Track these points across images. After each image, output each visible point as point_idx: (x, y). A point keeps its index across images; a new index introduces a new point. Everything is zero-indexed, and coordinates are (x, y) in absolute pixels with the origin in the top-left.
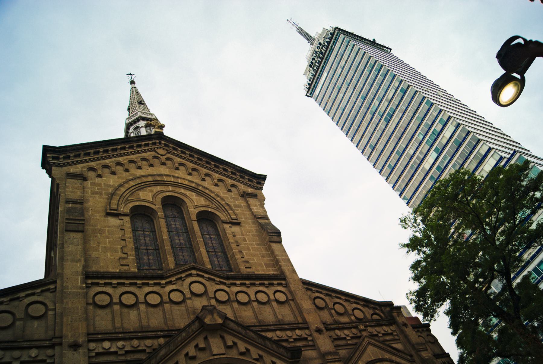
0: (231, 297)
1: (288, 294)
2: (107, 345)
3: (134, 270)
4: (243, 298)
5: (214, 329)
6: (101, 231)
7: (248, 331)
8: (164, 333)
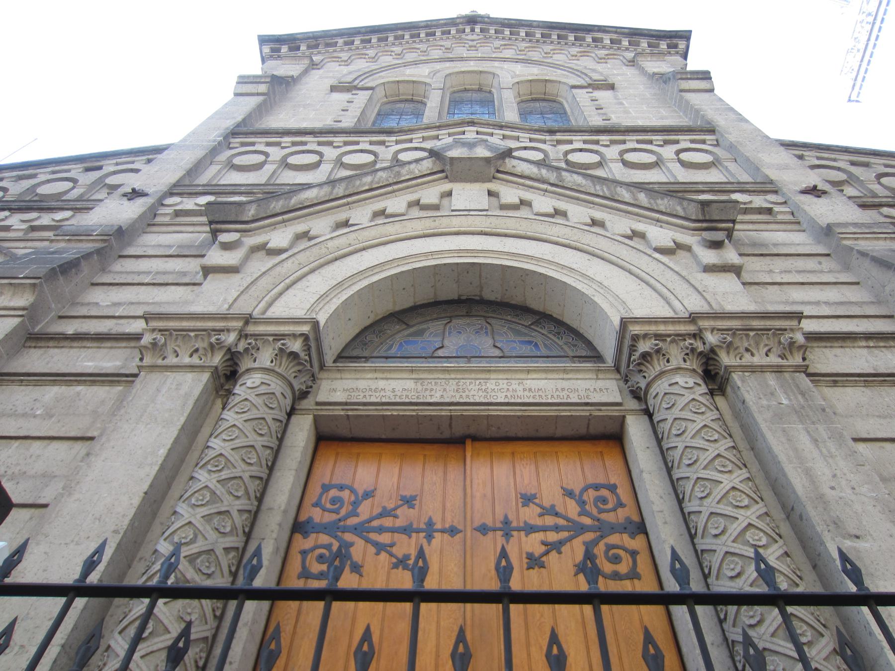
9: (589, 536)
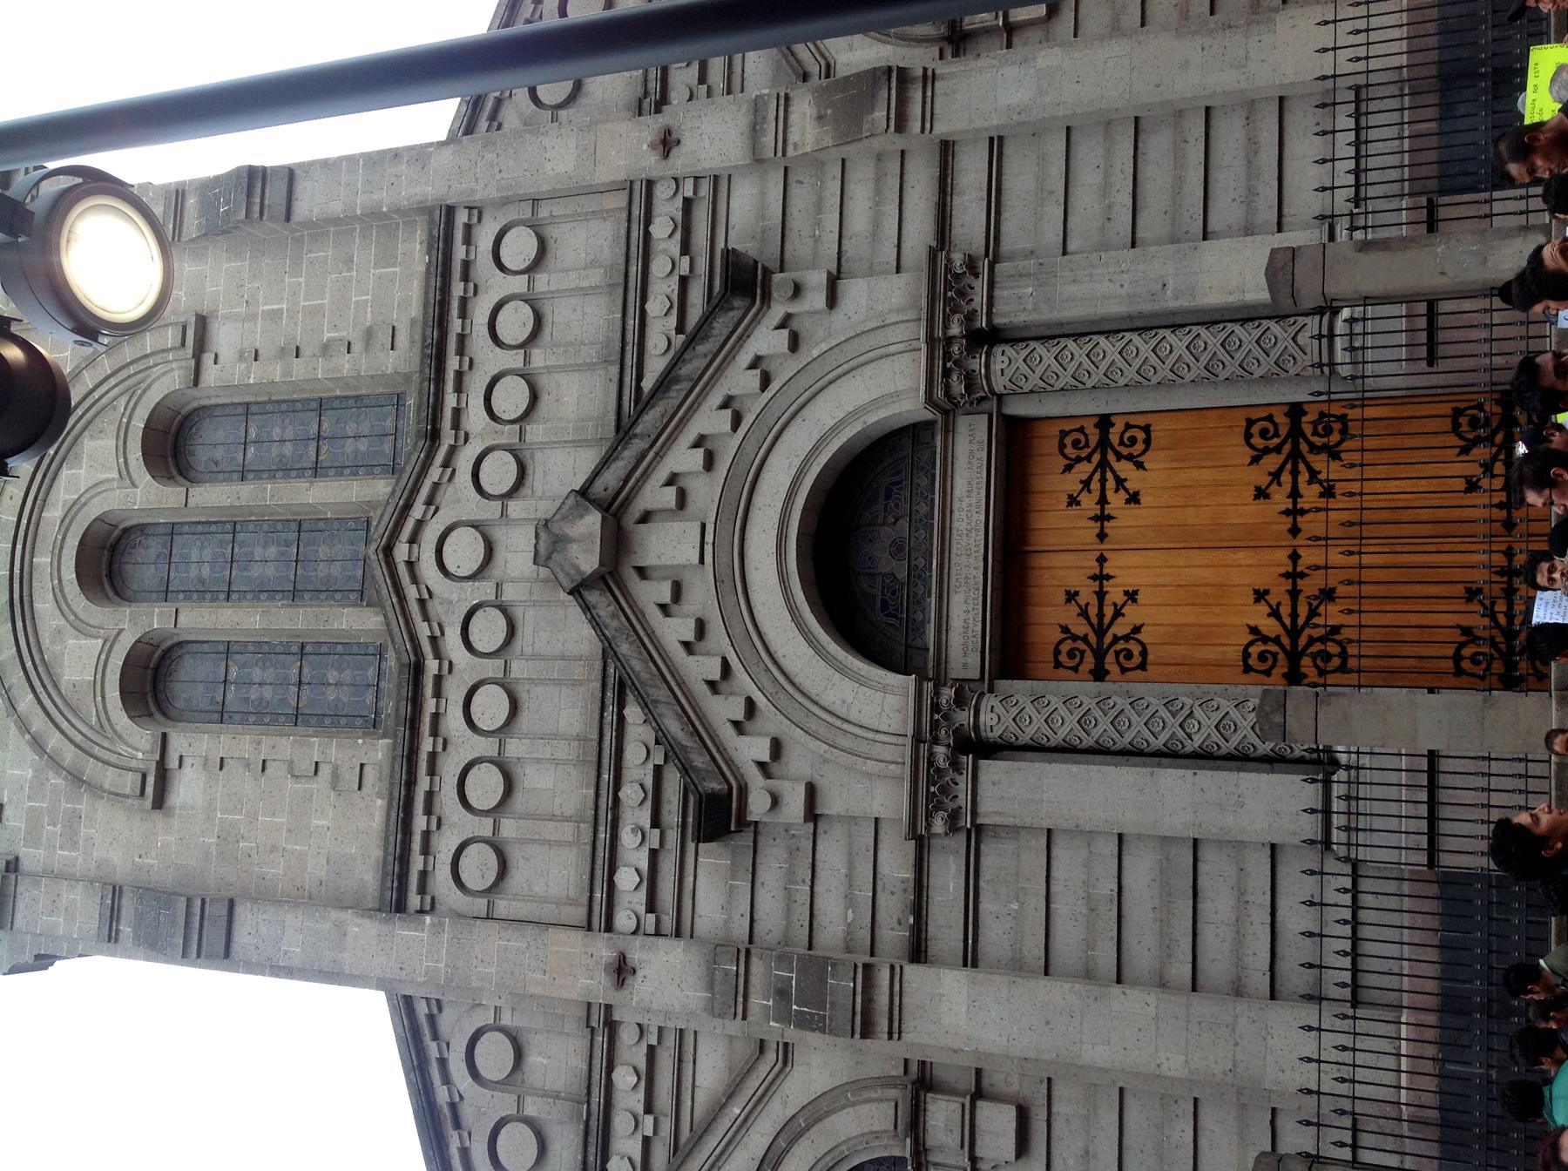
0: (503, 441)
1: (512, 214)
2: (626, 879)
3: (378, 752)
4: (510, 399)
5: (617, 542)
6: (228, 836)
7: (638, 430)
8: (609, 701)
9: (1111, 457)
